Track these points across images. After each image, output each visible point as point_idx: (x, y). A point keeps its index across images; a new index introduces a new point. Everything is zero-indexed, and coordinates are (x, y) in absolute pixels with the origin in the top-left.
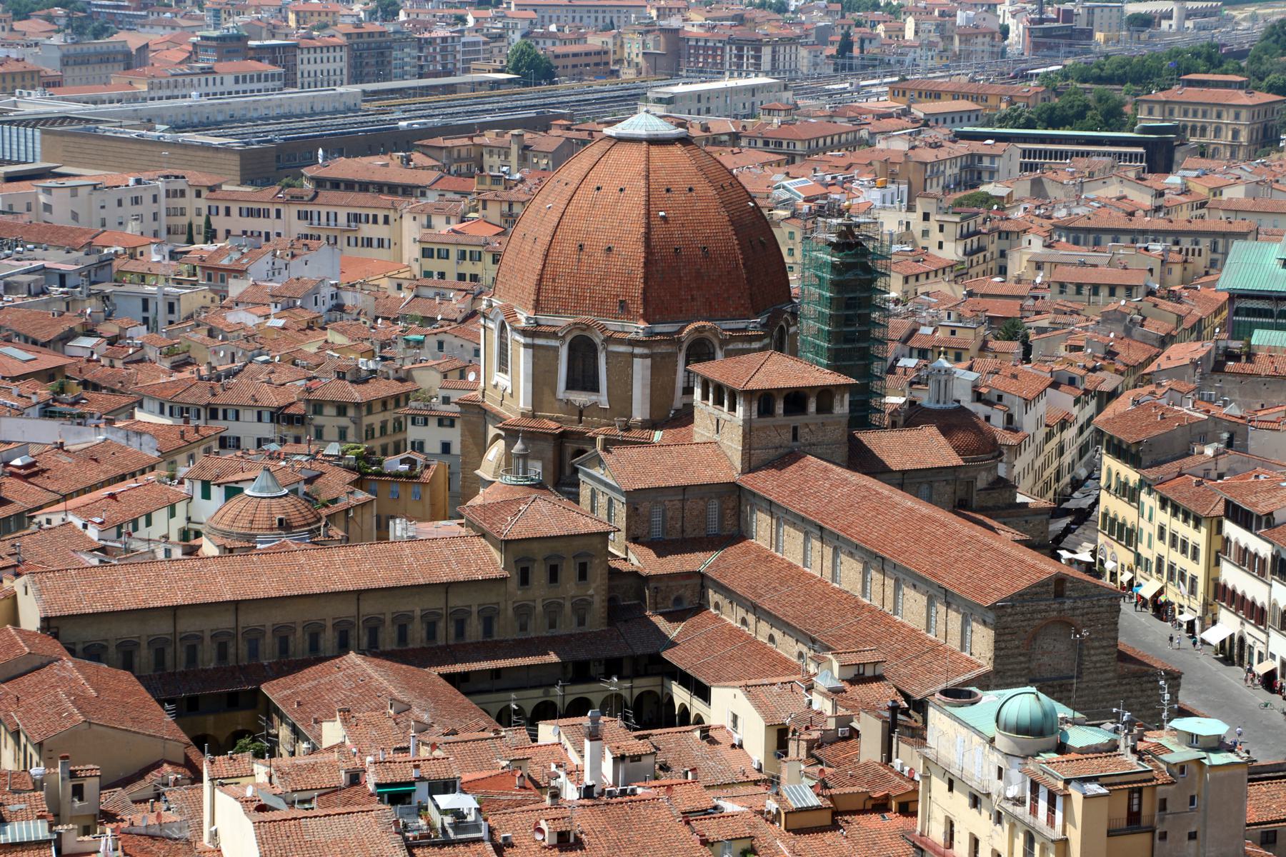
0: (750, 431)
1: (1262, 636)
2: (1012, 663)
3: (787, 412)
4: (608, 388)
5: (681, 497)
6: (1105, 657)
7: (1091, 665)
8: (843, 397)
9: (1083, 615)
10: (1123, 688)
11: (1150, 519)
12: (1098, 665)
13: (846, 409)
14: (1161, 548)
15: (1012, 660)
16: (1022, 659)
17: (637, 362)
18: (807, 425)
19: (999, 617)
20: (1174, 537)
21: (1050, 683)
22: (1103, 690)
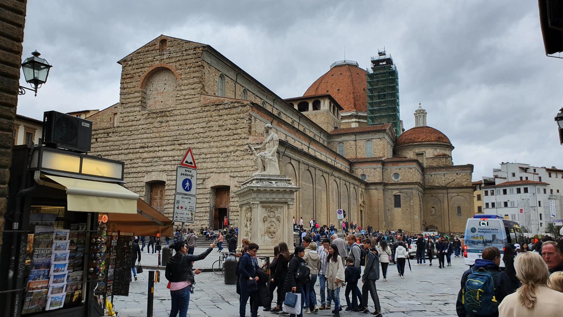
8: (324, 102)
9: (175, 62)
10: (205, 114)
12: (187, 97)
15: (131, 96)
16: (137, 94)
22: (191, 116)
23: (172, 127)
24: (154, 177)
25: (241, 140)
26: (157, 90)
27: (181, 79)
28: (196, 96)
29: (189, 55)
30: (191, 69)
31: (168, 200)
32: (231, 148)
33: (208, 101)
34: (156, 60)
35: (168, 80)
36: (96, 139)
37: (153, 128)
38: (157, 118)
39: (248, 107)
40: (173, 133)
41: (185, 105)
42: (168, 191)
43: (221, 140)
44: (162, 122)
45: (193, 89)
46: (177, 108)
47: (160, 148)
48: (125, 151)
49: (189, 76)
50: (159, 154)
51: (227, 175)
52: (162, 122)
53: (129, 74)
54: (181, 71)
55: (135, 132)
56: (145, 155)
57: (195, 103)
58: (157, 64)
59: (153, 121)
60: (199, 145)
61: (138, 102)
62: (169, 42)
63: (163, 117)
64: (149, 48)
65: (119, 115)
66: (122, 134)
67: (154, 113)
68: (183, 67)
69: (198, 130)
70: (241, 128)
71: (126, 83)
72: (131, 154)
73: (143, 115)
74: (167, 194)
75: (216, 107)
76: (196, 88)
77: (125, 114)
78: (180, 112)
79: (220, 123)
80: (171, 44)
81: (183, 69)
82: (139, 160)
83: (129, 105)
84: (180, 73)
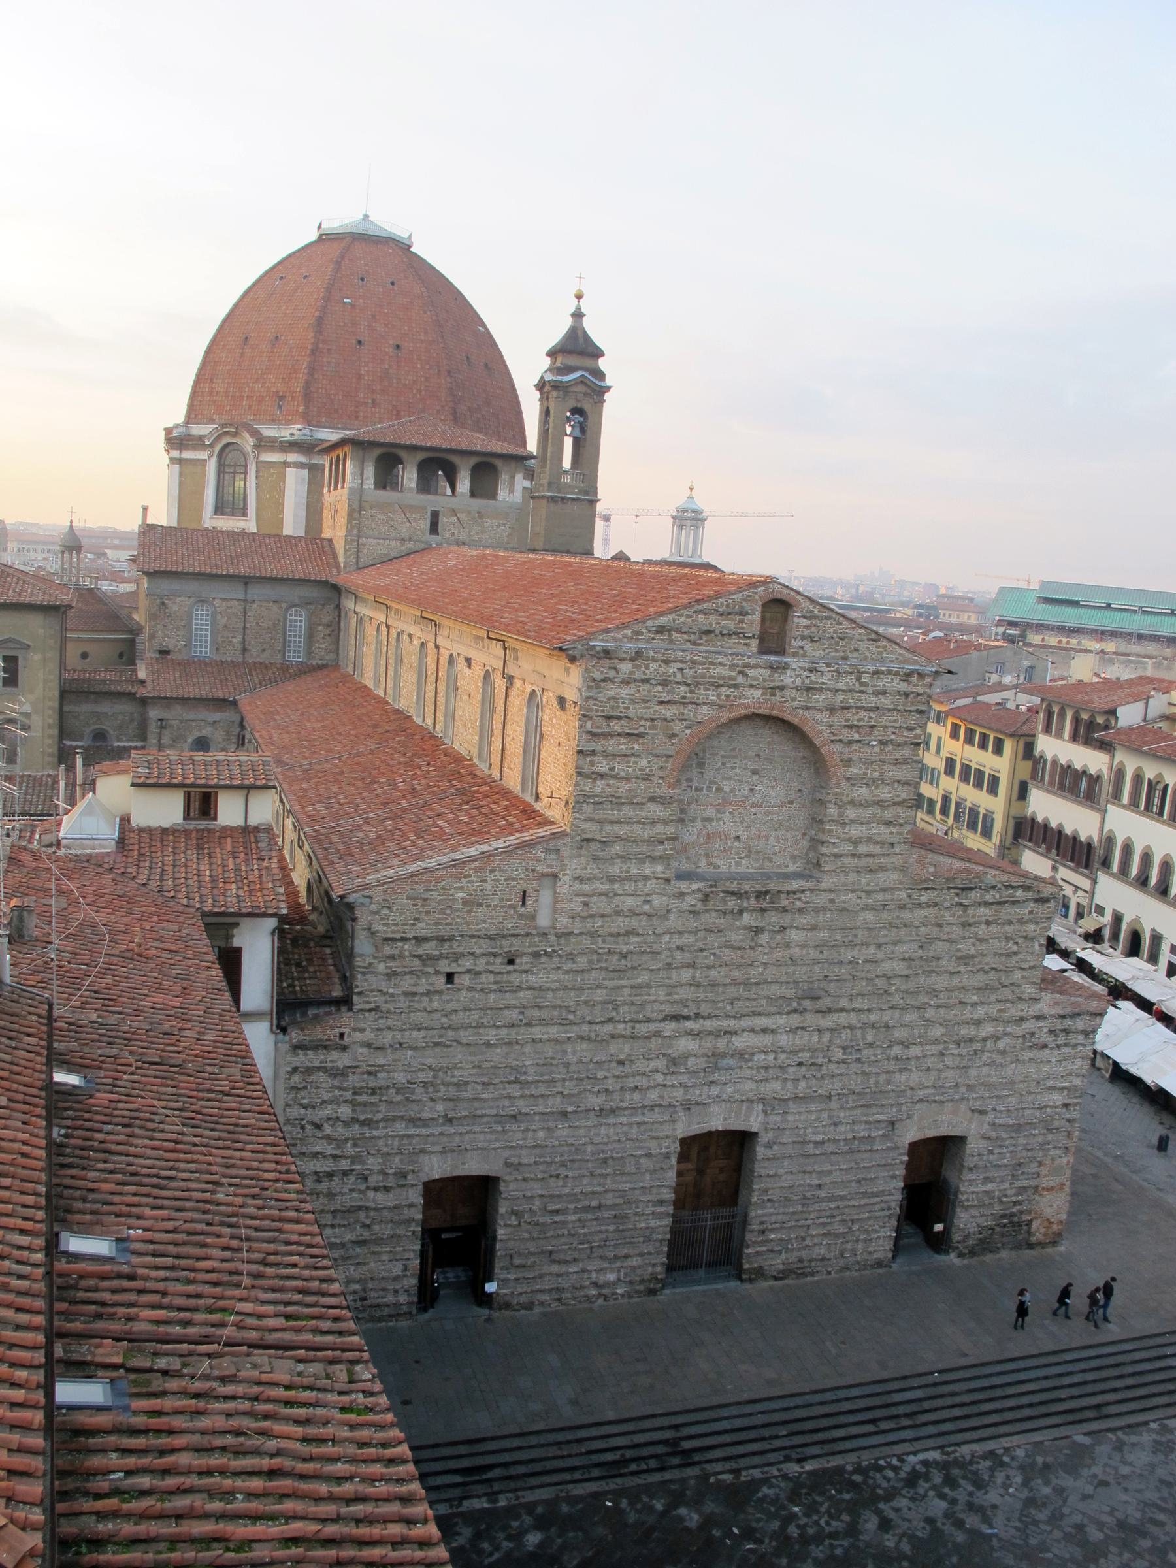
0: (361, 508)
1: (1086, 884)
2: (629, 821)
3: (425, 485)
4: (258, 509)
5: (241, 597)
6: (882, 829)
7: (845, 848)
8: (513, 477)
10: (920, 914)
11: (938, 751)
12: (863, 849)
13: (518, 496)
14: (950, 784)
15: (627, 811)
16: (656, 810)
17: (290, 472)
18: (454, 512)
19: (594, 683)
20: (966, 769)
21: (733, 887)
22: (869, 916)
23: (796, 951)
24: (717, 1120)
25: (1021, 1005)
26: (719, 789)
27: (848, 779)
28: (897, 849)
29: (884, 693)
30: (886, 750)
31: (766, 1191)
32: (988, 1029)
33: (932, 869)
34: (751, 686)
35: (770, 760)
36: (450, 977)
37: (719, 947)
38: (741, 912)
39: (1052, 904)
40: (801, 973)
41: (853, 876)
42: (766, 1164)
43: (961, 1003)
44: (759, 931)
45: (888, 823)
46: (823, 885)
47: (745, 1023)
48: (598, 1027)
49: (876, 774)
50: (739, 1042)
51: (963, 1107)
52: (759, 931)
53: (619, 718)
54: (847, 750)
55: (645, 958)
56: (685, 1045)
57: (887, 873)
58: (753, 699)
59: (721, 921)
60: (887, 1017)
61: (662, 843)
62: (805, 617)
63: (763, 910)
64: (711, 617)
65: (565, 885)
66: (582, 961)
67: (733, 893)
68: (856, 736)
69: (888, 967)
70: (1021, 969)
71: (606, 754)
72: (620, 1040)
73: (681, 895)
74: (763, 1172)
75: (957, 895)
76: (902, 821)
77: (598, 885)
78: (832, 901)
79: (966, 947)
80: (807, 627)
81: (858, 741)
82: (661, 1064)
83: (617, 848)
84: (845, 757)
